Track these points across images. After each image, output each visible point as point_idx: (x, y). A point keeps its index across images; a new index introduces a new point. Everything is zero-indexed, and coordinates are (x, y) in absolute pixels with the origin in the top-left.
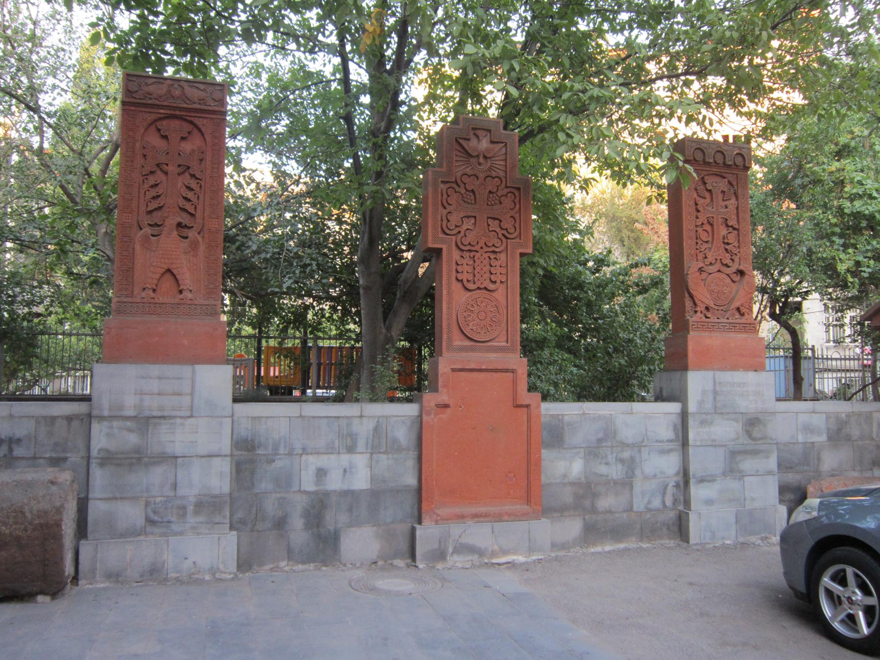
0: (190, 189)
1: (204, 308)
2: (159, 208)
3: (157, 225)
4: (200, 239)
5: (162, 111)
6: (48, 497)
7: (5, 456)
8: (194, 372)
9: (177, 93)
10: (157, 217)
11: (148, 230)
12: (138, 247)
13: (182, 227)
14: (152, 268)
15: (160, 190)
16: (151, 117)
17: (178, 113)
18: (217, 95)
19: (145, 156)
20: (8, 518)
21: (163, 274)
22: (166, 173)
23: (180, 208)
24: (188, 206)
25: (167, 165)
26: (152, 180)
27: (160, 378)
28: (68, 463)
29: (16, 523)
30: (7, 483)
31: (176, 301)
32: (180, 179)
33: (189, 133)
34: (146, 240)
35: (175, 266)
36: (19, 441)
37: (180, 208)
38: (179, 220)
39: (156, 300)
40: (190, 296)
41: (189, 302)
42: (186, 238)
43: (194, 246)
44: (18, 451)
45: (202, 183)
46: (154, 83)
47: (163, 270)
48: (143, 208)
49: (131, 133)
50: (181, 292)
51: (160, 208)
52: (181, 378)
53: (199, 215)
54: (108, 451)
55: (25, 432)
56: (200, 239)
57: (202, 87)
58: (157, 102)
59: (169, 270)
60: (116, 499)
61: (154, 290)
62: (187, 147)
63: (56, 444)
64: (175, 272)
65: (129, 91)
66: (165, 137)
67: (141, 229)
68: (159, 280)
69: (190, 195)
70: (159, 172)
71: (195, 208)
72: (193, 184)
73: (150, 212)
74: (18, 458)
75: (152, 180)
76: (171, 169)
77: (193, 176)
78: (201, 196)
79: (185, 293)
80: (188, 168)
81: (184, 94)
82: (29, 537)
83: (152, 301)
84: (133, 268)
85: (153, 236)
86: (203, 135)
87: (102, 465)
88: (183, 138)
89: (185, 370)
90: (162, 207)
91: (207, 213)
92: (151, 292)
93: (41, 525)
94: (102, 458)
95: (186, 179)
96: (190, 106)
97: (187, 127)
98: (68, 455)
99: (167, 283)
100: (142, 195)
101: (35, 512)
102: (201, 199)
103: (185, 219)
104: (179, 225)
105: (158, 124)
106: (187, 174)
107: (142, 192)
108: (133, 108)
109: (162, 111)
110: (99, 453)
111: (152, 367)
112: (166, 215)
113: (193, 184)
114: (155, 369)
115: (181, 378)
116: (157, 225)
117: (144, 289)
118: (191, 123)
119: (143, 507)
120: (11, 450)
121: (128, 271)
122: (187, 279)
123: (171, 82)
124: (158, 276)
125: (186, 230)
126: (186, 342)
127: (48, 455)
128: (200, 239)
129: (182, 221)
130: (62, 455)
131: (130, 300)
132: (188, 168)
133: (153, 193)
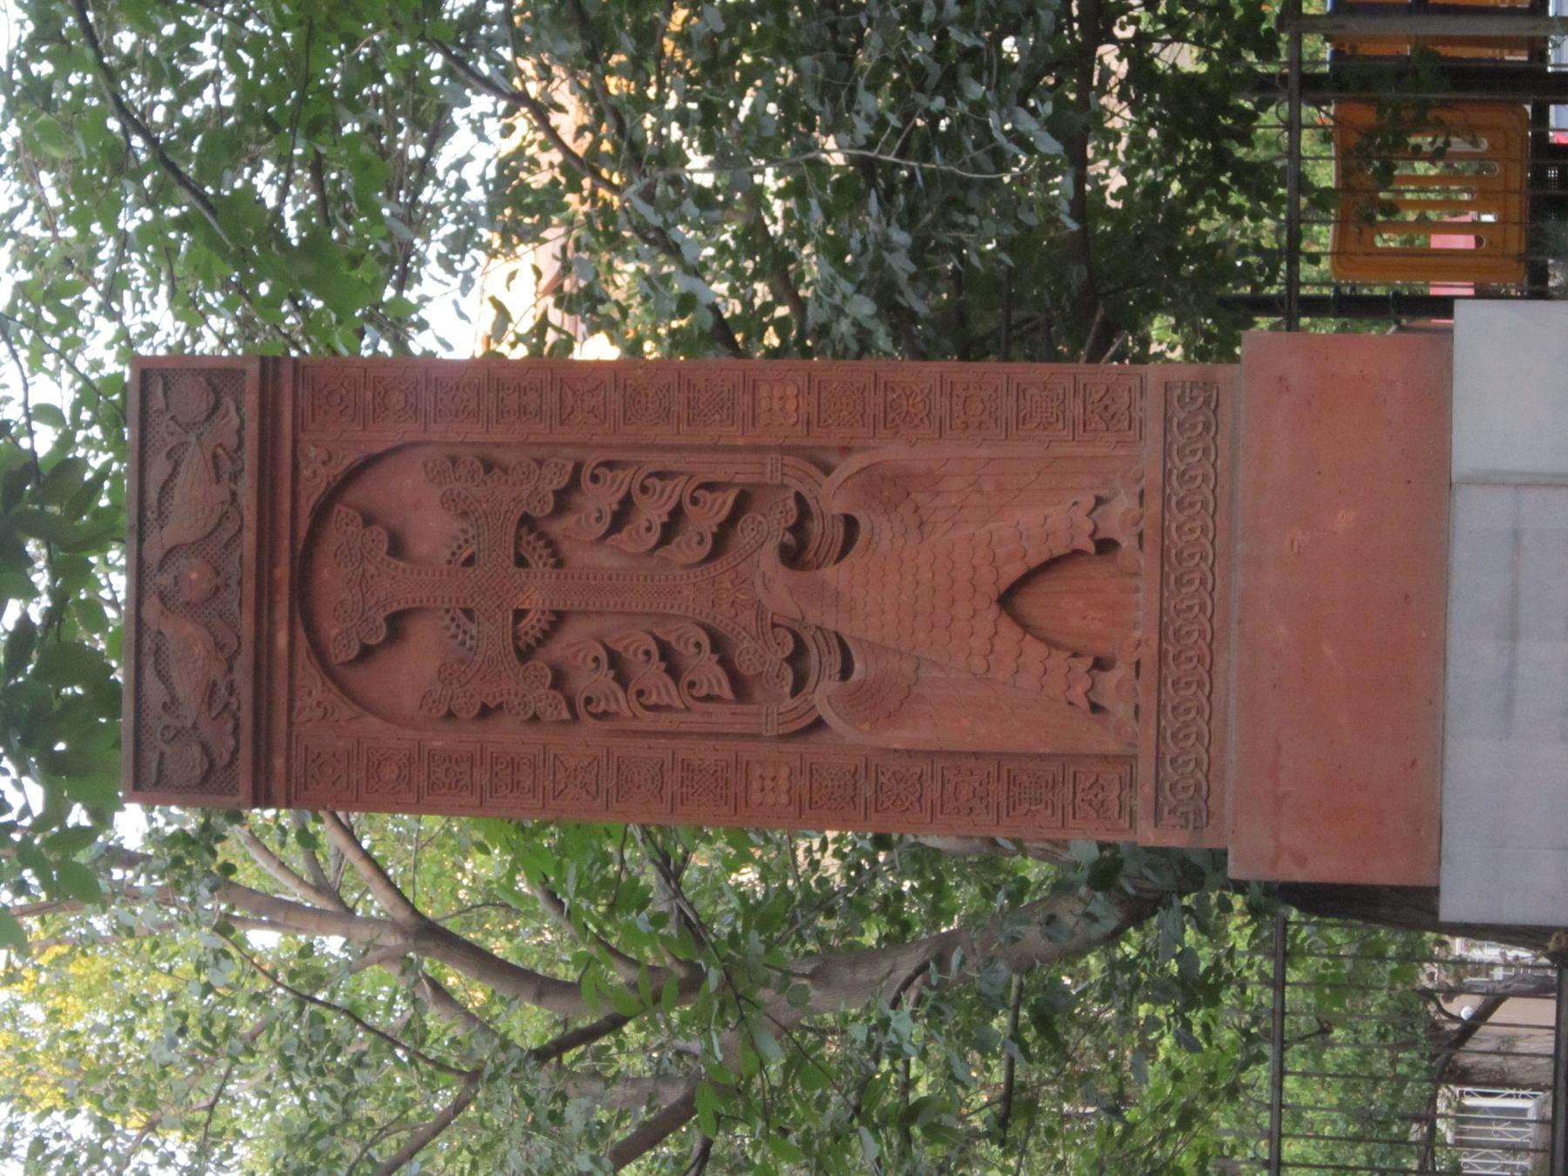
0: (622, 516)
2: (718, 644)
3: (798, 656)
4: (856, 462)
5: (282, 639)
8: (1485, 480)
9: (194, 573)
10: (761, 656)
11: (824, 694)
12: (899, 737)
13: (802, 545)
15: (635, 642)
16: (314, 689)
17: (283, 572)
18: (192, 401)
19: (485, 712)
21: (1026, 628)
22: (559, 618)
23: (713, 556)
25: (520, 614)
26: (592, 680)
27: (1512, 632)
31: (1147, 562)
32: (581, 557)
33: (369, 520)
37: (713, 556)
38: (768, 558)
39: (1148, 654)
40: (1123, 504)
41: (1154, 506)
42: (851, 524)
43: (891, 488)
45: (592, 459)
46: (162, 675)
48: (723, 717)
49: (390, 772)
50: (1106, 546)
51: (718, 644)
52: (1516, 535)
53: (741, 472)
56: (847, 467)
57: (158, 469)
58: (245, 661)
59: (1007, 599)
61: (1101, 664)
62: (433, 531)
64: (1013, 571)
65: (205, 779)
66: (397, 624)
67: (819, 724)
68: (1051, 644)
69: (652, 512)
70: (558, 650)
71: (710, 486)
72: (600, 499)
73: (740, 686)
75: (592, 680)
76: (537, 595)
77: (563, 501)
78: (656, 461)
80: (526, 521)
81: (196, 547)
83: (1148, 669)
84: (999, 757)
85: (846, 671)
86: (370, 462)
88: (397, 547)
89: (1476, 518)
90: (710, 631)
92: (1109, 679)
95: (579, 528)
96: (250, 518)
97: (342, 532)
99: (1064, 606)
100: (664, 721)
102: (669, 461)
103: (764, 533)
104: (794, 556)
105: (339, 654)
106: (557, 528)
107: (648, 721)
108: (279, 762)
109: (282, 639)
111: (1458, 669)
112: (748, 617)
113: (600, 499)
114: (1471, 656)
115: (1516, 535)
116: (798, 656)
117: (1095, 708)
118: (322, 513)
121: (1012, 780)
122: (1045, 521)
123: (155, 599)
124: (1035, 650)
125: (816, 527)
126: (1342, 521)
128: (856, 462)
129: (772, 546)
131: (1145, 770)
132: (526, 521)
133: (651, 675)
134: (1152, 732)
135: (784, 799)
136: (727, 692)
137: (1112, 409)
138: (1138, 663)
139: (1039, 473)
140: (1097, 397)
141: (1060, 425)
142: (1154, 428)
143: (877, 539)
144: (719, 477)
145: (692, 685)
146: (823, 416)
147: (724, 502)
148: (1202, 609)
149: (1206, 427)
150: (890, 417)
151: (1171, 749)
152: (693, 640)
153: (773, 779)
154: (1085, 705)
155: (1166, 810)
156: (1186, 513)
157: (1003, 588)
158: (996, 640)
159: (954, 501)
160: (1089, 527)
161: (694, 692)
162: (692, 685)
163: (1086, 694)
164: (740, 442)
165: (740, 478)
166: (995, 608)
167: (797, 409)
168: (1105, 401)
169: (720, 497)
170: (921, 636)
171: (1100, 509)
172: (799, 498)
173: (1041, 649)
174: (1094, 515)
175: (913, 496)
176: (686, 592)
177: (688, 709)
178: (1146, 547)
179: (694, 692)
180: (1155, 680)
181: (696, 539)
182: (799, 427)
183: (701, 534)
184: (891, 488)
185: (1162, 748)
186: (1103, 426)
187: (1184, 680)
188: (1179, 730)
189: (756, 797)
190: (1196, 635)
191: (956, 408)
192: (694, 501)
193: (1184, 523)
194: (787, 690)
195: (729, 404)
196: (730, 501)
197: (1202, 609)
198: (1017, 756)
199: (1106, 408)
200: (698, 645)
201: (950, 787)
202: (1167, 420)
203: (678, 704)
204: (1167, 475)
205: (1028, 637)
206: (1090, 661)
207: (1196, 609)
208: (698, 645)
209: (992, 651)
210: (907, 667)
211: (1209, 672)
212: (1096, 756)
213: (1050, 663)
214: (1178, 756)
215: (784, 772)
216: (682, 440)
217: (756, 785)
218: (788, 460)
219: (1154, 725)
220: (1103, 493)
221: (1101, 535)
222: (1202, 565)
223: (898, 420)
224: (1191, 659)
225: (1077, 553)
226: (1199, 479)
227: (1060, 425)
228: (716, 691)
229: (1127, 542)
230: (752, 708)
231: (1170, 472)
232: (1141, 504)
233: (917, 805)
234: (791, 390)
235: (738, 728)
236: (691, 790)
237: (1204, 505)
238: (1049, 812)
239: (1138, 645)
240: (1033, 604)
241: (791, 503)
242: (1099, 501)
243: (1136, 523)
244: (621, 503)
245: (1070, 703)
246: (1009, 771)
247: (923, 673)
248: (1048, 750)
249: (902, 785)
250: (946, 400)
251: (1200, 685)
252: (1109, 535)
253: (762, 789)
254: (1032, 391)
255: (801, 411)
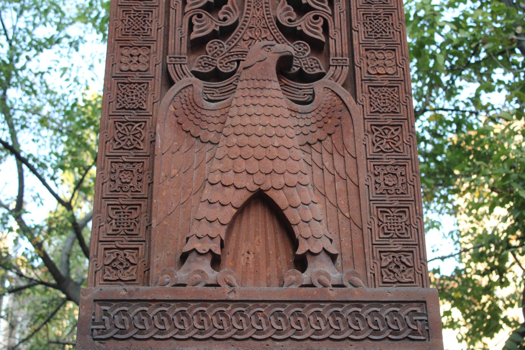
1: (385, 312)
2: (225, 33)
3: (217, 76)
10: (218, 54)
12: (166, 136)
14: (208, 193)
21: (242, 210)
24: (303, 24)
34: (192, 107)
35: (278, 181)
40: (334, 275)
41: (333, 294)
47: (239, 198)
48: (179, 41)
50: (301, 263)
51: (225, 33)
53: (337, 44)
59: (261, 199)
61: (216, 262)
64: (280, 199)
68: (230, 226)
73: (197, 45)
79: (320, 269)
83: (213, 293)
84: (149, 198)
91: (359, 38)
92: (205, 265)
99: (257, 236)
116: (217, 76)
117: (184, 257)
128: (348, 98)
134: (166, 297)
135: (124, 68)
136: (193, 36)
137: (396, 270)
138: (218, 285)
139: (349, 219)
140: (404, 260)
141: (382, 235)
142: (392, 292)
143: (298, 116)
144: (331, 31)
145: (200, 16)
146: (376, 90)
147: (316, 34)
148: (258, 332)
149: (395, 332)
150: (380, 129)
151: (153, 311)
152: (228, 17)
153: (138, 61)
154: (187, 249)
155: (107, 308)
156: (330, 318)
157: (271, 194)
158: (232, 189)
159: (327, 164)
160: (315, 250)
161: (195, 17)
162: (200, 16)
163: (194, 250)
164: (355, 42)
165: (331, 42)
166: (255, 188)
167: (378, 74)
168: (402, 266)
169: (320, 31)
170: (234, 140)
171: (329, 258)
172: (321, 76)
173: (227, 220)
174: (323, 256)
175: (329, 138)
176: (258, 13)
177: (184, 14)
178: (303, 289)
179: (195, 17)
180: (205, 298)
181: (293, 18)
182: (367, 75)
183: (294, 21)
184: (332, 122)
185: (153, 304)
186: (384, 264)
187: (204, 319)
188: (168, 316)
189: (125, 52)
190: (240, 327)
191: (388, 168)
192: (316, 17)
193: (322, 316)
194: (197, 69)
195: (379, 36)
196: (316, 37)
197: (258, 332)
198: (150, 210)
199: (397, 267)
200: (225, 19)
201: (130, 167)
202: (398, 303)
203: (187, 9)
204: (358, 303)
205: (235, 211)
206: (218, 252)
207: (259, 327)
208: (225, 19)
209: (224, 186)
210: (212, 136)
211: (211, 338)
212: (149, 263)
213: (216, 225)
214: (148, 316)
215: (142, 68)
216: (353, 12)
217: (134, 52)
218: (346, 70)
219: (171, 298)
220: (338, 260)
221: (309, 258)
222: (293, 331)
223: (376, 133)
224: (221, 324)
225: (295, 243)
226: (356, 328)
227: (382, 235)
228: (195, 29)
229: (306, 277)
230: (184, 49)
231: (360, 307)
232: (333, 286)
233: (119, 146)
234: (390, 71)
235: (171, 42)
236: (132, 16)
237: (337, 332)
238: (110, 232)
239: (231, 285)
240: (258, 218)
241: (318, 71)
242: (333, 257)
243: (320, 282)
244: (307, 4)
245: (188, 239)
246: (140, 205)
247: (209, 146)
248: (154, 226)
249: (132, 138)
250: (392, 162)
251: (201, 331)
252: (310, 264)
253: (132, 56)
254: (405, 218)
255: (378, 77)
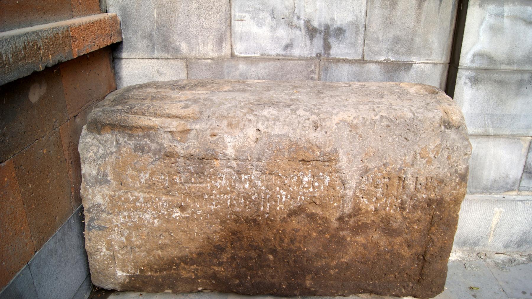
6: (446, 154)
7: (319, 56)
20: (376, 187)
28: (412, 71)
29: (387, 196)
30: (373, 123)
36: (340, 31)
44: (339, 50)
54: (491, 59)
55: (350, 18)
60: (488, 136)
63: (397, 40)
74: (338, 61)
82: (405, 218)
87: (475, 81)
93: (430, 202)
94: (477, 70)
98: (414, 59)
101: (422, 180)
110: (472, 61)
119: (524, 151)
120: (327, 46)
127: (382, 59)
130: (404, 59)
